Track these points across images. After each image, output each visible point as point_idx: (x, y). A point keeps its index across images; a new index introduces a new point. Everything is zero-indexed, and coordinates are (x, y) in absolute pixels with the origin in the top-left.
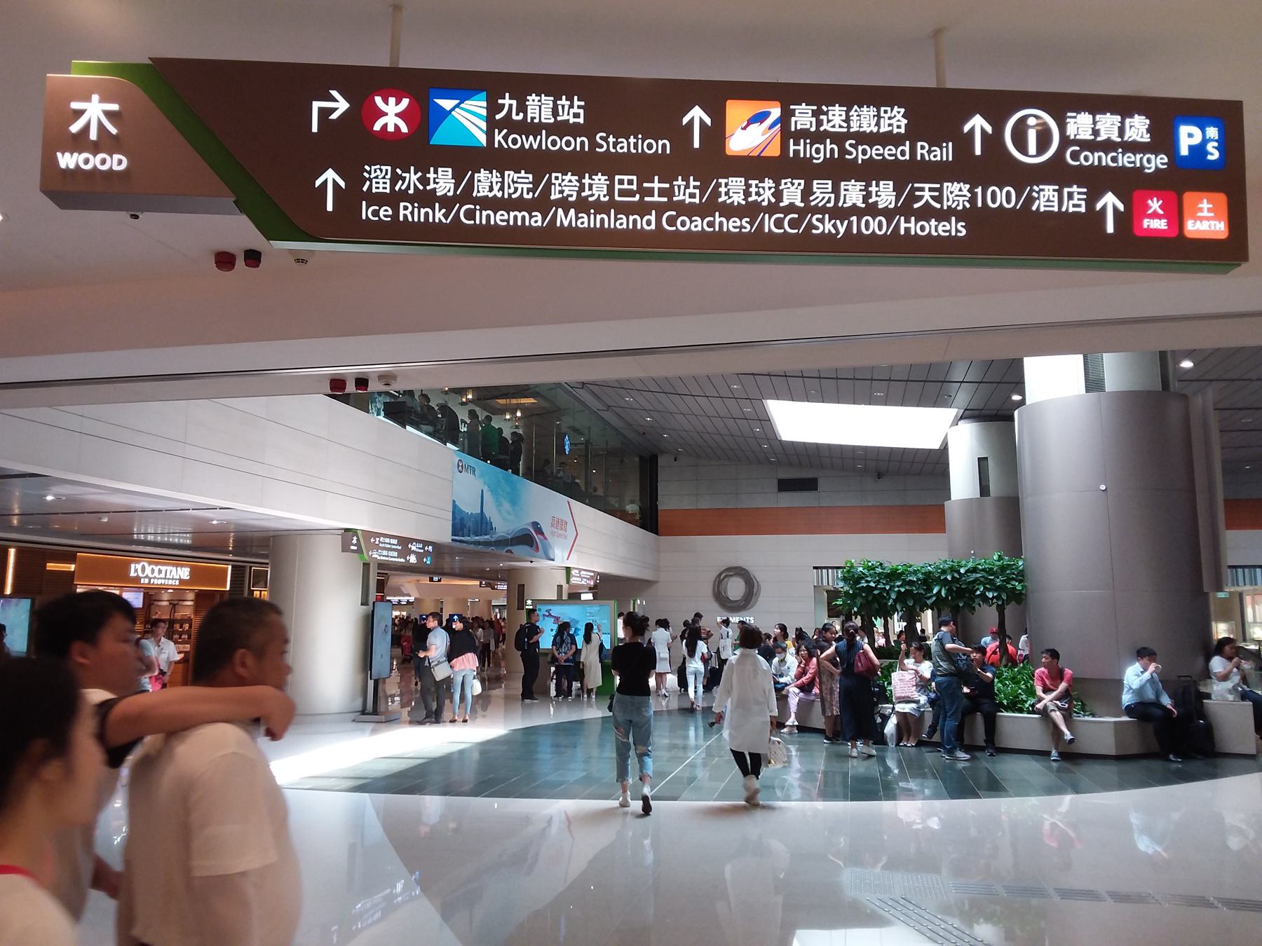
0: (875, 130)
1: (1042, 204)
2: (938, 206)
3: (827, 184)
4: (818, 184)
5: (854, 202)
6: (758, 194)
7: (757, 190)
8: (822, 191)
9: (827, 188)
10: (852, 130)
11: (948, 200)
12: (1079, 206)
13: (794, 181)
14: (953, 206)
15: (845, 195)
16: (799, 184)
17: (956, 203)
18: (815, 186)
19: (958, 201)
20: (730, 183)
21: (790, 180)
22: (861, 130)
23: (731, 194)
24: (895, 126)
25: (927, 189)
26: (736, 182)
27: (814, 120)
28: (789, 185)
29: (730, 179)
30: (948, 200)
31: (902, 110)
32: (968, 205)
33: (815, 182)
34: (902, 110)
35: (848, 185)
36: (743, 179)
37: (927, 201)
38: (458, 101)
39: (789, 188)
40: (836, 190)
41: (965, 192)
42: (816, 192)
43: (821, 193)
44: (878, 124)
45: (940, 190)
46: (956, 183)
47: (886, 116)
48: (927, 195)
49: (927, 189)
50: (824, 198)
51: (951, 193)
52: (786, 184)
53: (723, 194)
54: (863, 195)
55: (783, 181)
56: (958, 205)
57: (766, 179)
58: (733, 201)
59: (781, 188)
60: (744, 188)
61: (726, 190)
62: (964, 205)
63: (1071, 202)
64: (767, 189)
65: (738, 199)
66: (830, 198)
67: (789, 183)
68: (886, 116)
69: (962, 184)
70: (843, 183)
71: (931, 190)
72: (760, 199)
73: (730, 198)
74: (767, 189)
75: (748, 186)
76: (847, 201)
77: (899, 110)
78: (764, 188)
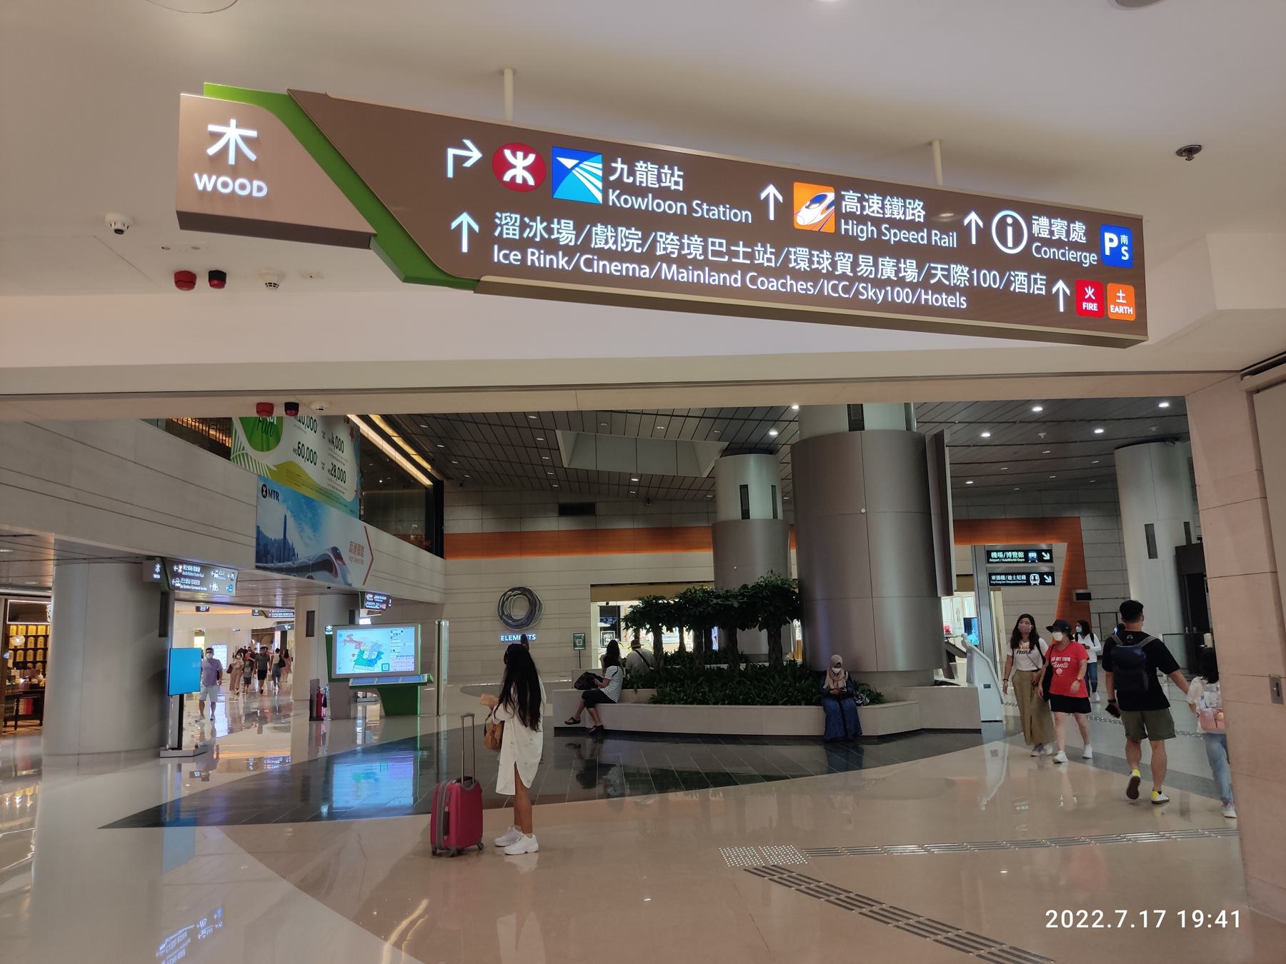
1: (1017, 286)
5: (889, 275)
6: (819, 263)
8: (865, 265)
9: (869, 262)
11: (954, 279)
12: (1041, 289)
13: (846, 254)
14: (958, 284)
15: (882, 269)
16: (849, 257)
18: (861, 260)
20: (798, 252)
23: (799, 262)
25: (939, 269)
28: (842, 257)
29: (798, 249)
30: (954, 279)
33: (861, 256)
36: (807, 250)
39: (841, 260)
40: (875, 264)
41: (966, 274)
43: (865, 266)
50: (867, 270)
51: (956, 273)
54: (895, 270)
55: (837, 254)
57: (825, 251)
63: (1036, 286)
64: (825, 259)
65: (804, 266)
66: (871, 270)
70: (880, 259)
72: (820, 268)
73: (798, 264)
74: (825, 259)
75: (811, 255)
76: (884, 274)
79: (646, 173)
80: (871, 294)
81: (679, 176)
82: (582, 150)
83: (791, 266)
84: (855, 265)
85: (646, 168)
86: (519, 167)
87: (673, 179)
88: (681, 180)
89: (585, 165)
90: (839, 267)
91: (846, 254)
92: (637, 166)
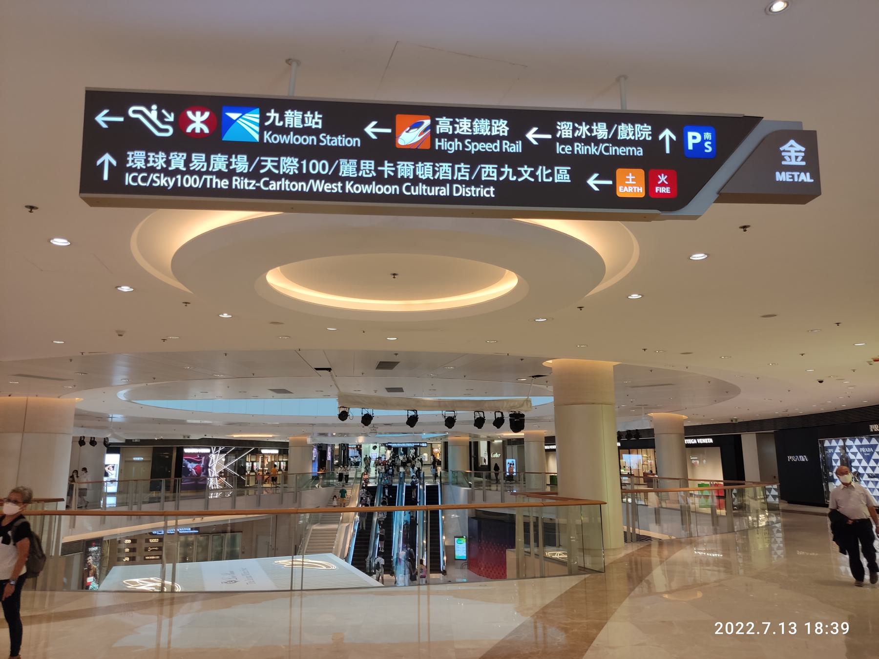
0: (489, 134)
1: (441, 175)
4: (195, 156)
7: (153, 159)
9: (202, 159)
10: (474, 134)
11: (283, 168)
12: (465, 176)
16: (183, 156)
17: (289, 170)
19: (290, 169)
22: (480, 133)
24: (501, 132)
25: (269, 161)
26: (140, 154)
27: (451, 127)
30: (283, 168)
31: (506, 122)
32: (297, 172)
34: (506, 122)
35: (216, 157)
38: (240, 115)
43: (198, 162)
44: (490, 130)
45: (278, 162)
47: (496, 125)
49: (269, 161)
50: (199, 165)
51: (286, 163)
52: (173, 155)
56: (290, 171)
61: (133, 159)
63: (460, 174)
67: (176, 156)
68: (496, 125)
71: (272, 161)
77: (504, 122)
78: (158, 158)
79: (293, 118)
81: (319, 118)
82: (244, 104)
83: (128, 165)
85: (293, 114)
86: (198, 122)
87: (314, 121)
88: (320, 121)
89: (247, 116)
91: (179, 154)
92: (286, 114)
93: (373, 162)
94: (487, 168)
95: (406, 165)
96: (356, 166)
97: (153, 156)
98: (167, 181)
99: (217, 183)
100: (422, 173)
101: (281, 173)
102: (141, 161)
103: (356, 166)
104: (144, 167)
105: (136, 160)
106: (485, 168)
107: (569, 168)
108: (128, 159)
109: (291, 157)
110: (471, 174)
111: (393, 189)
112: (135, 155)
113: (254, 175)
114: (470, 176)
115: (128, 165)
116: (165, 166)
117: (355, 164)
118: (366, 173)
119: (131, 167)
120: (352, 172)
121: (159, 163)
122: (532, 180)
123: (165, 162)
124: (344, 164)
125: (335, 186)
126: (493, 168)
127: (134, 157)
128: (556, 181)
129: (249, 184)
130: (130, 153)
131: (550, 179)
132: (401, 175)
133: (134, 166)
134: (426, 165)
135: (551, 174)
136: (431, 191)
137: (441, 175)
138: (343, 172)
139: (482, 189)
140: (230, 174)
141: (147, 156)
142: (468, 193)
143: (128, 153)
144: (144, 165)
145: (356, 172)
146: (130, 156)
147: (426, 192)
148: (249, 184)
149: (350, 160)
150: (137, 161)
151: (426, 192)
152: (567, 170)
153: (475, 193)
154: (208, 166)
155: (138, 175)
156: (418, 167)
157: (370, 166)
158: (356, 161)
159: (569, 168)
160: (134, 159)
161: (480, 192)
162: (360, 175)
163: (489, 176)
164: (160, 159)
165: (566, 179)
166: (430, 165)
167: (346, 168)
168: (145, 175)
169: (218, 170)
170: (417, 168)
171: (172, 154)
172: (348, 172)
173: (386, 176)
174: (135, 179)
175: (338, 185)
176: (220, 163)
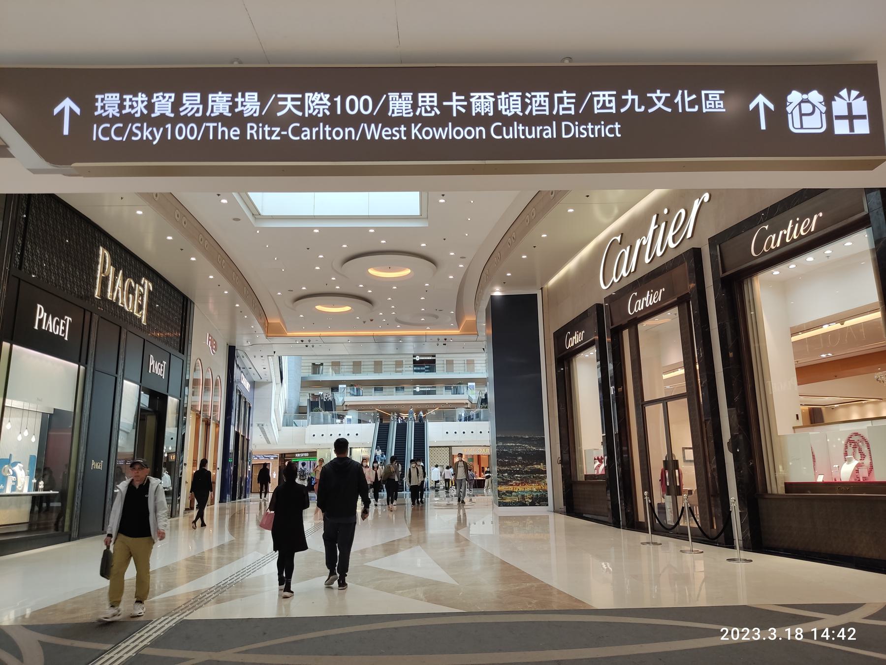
2: (300, 114)
3: (196, 96)
9: (196, 100)
11: (309, 108)
13: (165, 95)
16: (170, 97)
18: (185, 98)
19: (319, 109)
21: (161, 94)
25: (289, 99)
28: (161, 98)
30: (309, 108)
32: (328, 113)
33: (185, 95)
35: (216, 97)
37: (290, 109)
39: (160, 101)
40: (204, 101)
41: (325, 101)
42: (185, 104)
43: (190, 104)
45: (302, 100)
46: (316, 93)
48: (289, 104)
49: (289, 99)
50: (192, 109)
51: (313, 102)
52: (157, 97)
53: (99, 108)
54: (230, 106)
56: (319, 113)
58: (109, 114)
59: (153, 101)
60: (119, 102)
61: (102, 104)
62: (324, 113)
66: (198, 109)
69: (322, 94)
71: (293, 99)
78: (137, 102)
80: (146, 133)
83: (96, 113)
84: (177, 104)
90: (156, 109)
93: (435, 95)
94: (601, 96)
95: (482, 97)
96: (412, 102)
97: (130, 100)
98: (152, 133)
99: (223, 132)
100: (507, 107)
101: (307, 115)
102: (115, 107)
103: (412, 102)
104: (118, 115)
105: (107, 106)
106: (598, 96)
107: (723, 92)
108: (96, 104)
109: (319, 93)
110: (577, 106)
111: (477, 132)
112: (106, 99)
113: (267, 118)
114: (577, 110)
115: (96, 113)
116: (145, 112)
117: (410, 99)
118: (426, 111)
119: (101, 115)
120: (406, 110)
121: (138, 109)
122: (669, 110)
123: (145, 107)
124: (394, 99)
125: (396, 131)
126: (610, 95)
127: (104, 102)
128: (705, 110)
129: (271, 133)
130: (99, 97)
131: (696, 108)
132: (476, 112)
133: (104, 115)
134: (512, 96)
135: (697, 102)
136: (530, 134)
137: (534, 110)
138: (393, 111)
139: (603, 127)
140: (237, 119)
141: (122, 100)
142: (583, 134)
143: (97, 96)
144: (118, 112)
145: (411, 110)
146: (100, 100)
147: (524, 134)
148: (271, 133)
149: (402, 94)
150: (108, 107)
151: (524, 134)
152: (720, 94)
153: (593, 133)
154: (205, 109)
155: (111, 127)
156: (501, 99)
157: (431, 101)
158: (412, 94)
159: (723, 92)
160: (104, 104)
161: (600, 130)
162: (418, 113)
163: (604, 107)
164: (140, 102)
165: (719, 108)
166: (517, 96)
167: (397, 105)
168: (121, 125)
169: (218, 114)
170: (499, 101)
171: (155, 95)
172: (401, 111)
173: (455, 114)
174: (106, 132)
175: (401, 129)
176: (221, 104)
